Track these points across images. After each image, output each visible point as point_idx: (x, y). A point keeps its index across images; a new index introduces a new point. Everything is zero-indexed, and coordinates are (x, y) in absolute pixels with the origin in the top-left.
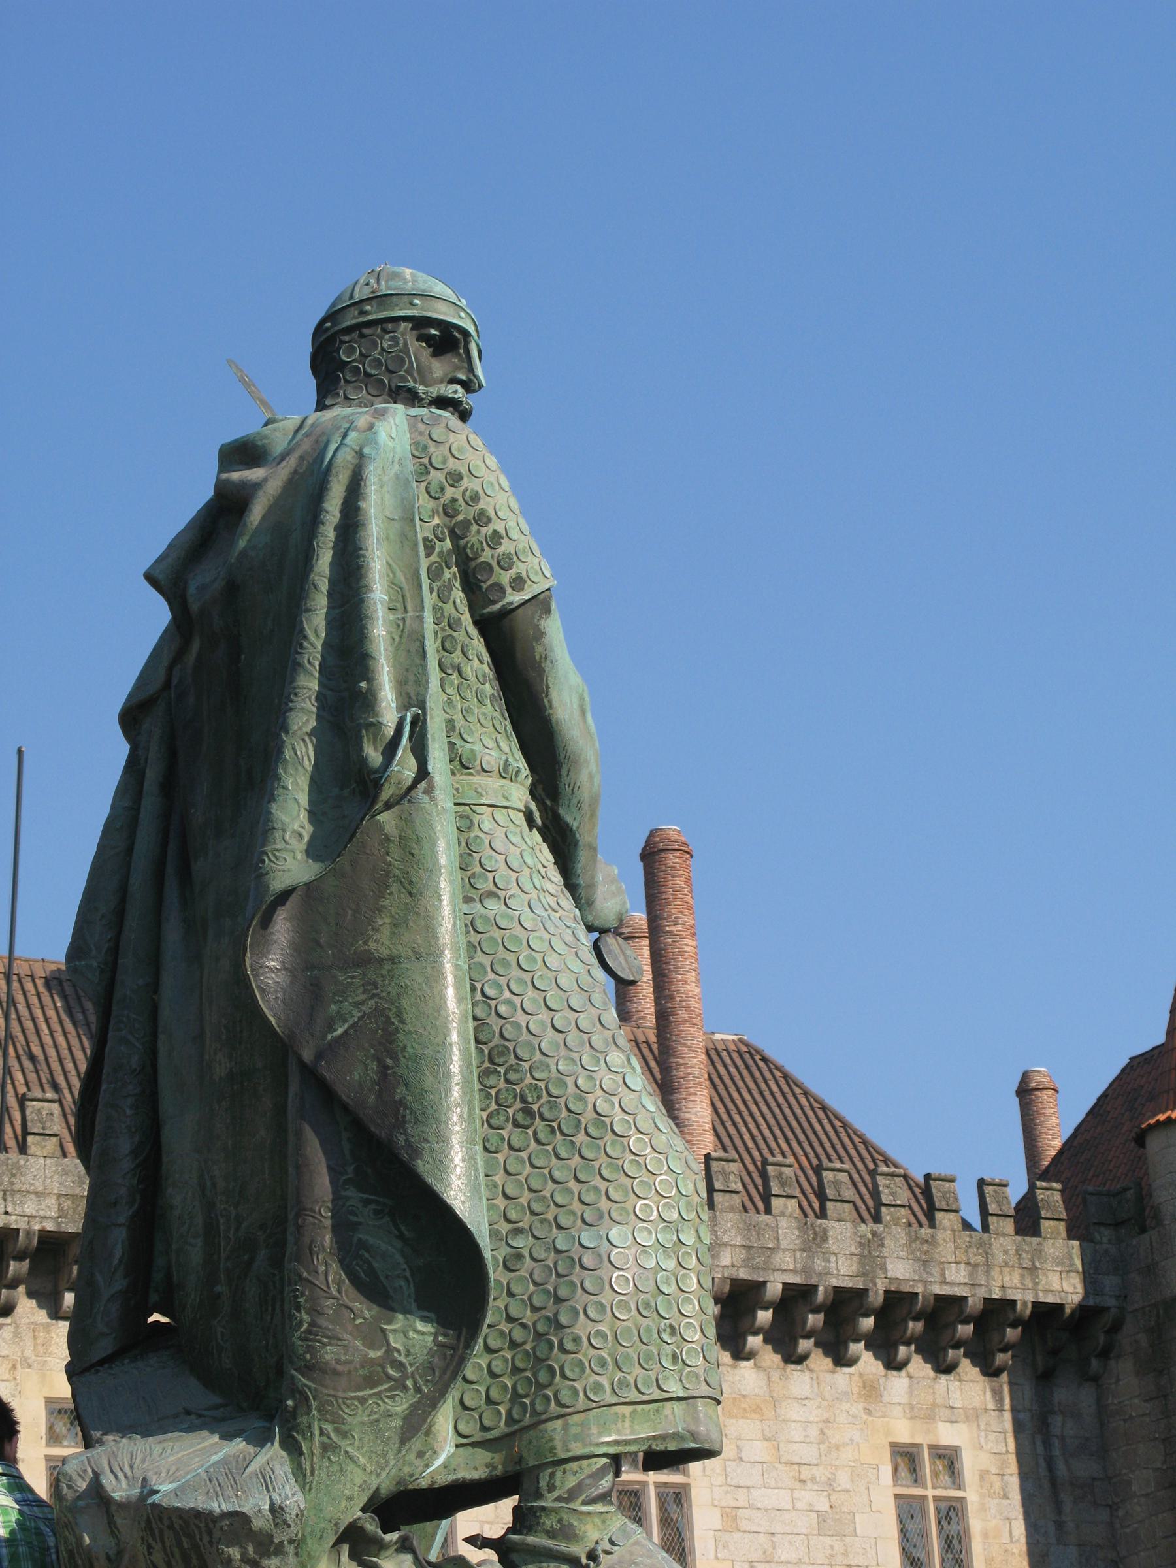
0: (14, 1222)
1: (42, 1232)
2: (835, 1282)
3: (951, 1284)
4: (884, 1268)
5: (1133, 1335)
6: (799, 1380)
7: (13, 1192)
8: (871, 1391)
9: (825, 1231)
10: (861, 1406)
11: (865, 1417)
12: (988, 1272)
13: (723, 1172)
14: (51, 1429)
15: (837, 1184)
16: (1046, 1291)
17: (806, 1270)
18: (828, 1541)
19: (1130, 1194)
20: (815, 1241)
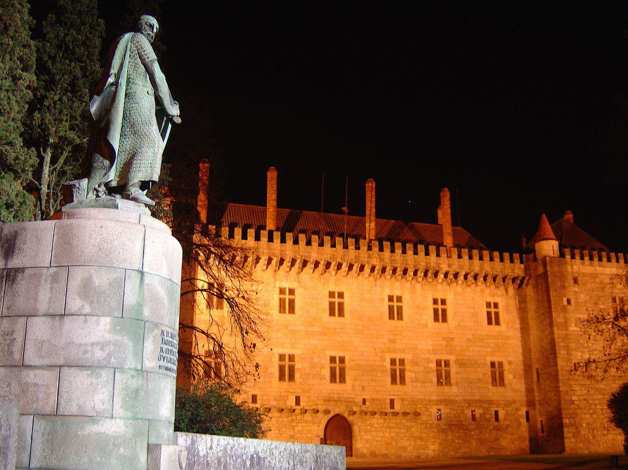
6: (469, 289)
8: (482, 291)
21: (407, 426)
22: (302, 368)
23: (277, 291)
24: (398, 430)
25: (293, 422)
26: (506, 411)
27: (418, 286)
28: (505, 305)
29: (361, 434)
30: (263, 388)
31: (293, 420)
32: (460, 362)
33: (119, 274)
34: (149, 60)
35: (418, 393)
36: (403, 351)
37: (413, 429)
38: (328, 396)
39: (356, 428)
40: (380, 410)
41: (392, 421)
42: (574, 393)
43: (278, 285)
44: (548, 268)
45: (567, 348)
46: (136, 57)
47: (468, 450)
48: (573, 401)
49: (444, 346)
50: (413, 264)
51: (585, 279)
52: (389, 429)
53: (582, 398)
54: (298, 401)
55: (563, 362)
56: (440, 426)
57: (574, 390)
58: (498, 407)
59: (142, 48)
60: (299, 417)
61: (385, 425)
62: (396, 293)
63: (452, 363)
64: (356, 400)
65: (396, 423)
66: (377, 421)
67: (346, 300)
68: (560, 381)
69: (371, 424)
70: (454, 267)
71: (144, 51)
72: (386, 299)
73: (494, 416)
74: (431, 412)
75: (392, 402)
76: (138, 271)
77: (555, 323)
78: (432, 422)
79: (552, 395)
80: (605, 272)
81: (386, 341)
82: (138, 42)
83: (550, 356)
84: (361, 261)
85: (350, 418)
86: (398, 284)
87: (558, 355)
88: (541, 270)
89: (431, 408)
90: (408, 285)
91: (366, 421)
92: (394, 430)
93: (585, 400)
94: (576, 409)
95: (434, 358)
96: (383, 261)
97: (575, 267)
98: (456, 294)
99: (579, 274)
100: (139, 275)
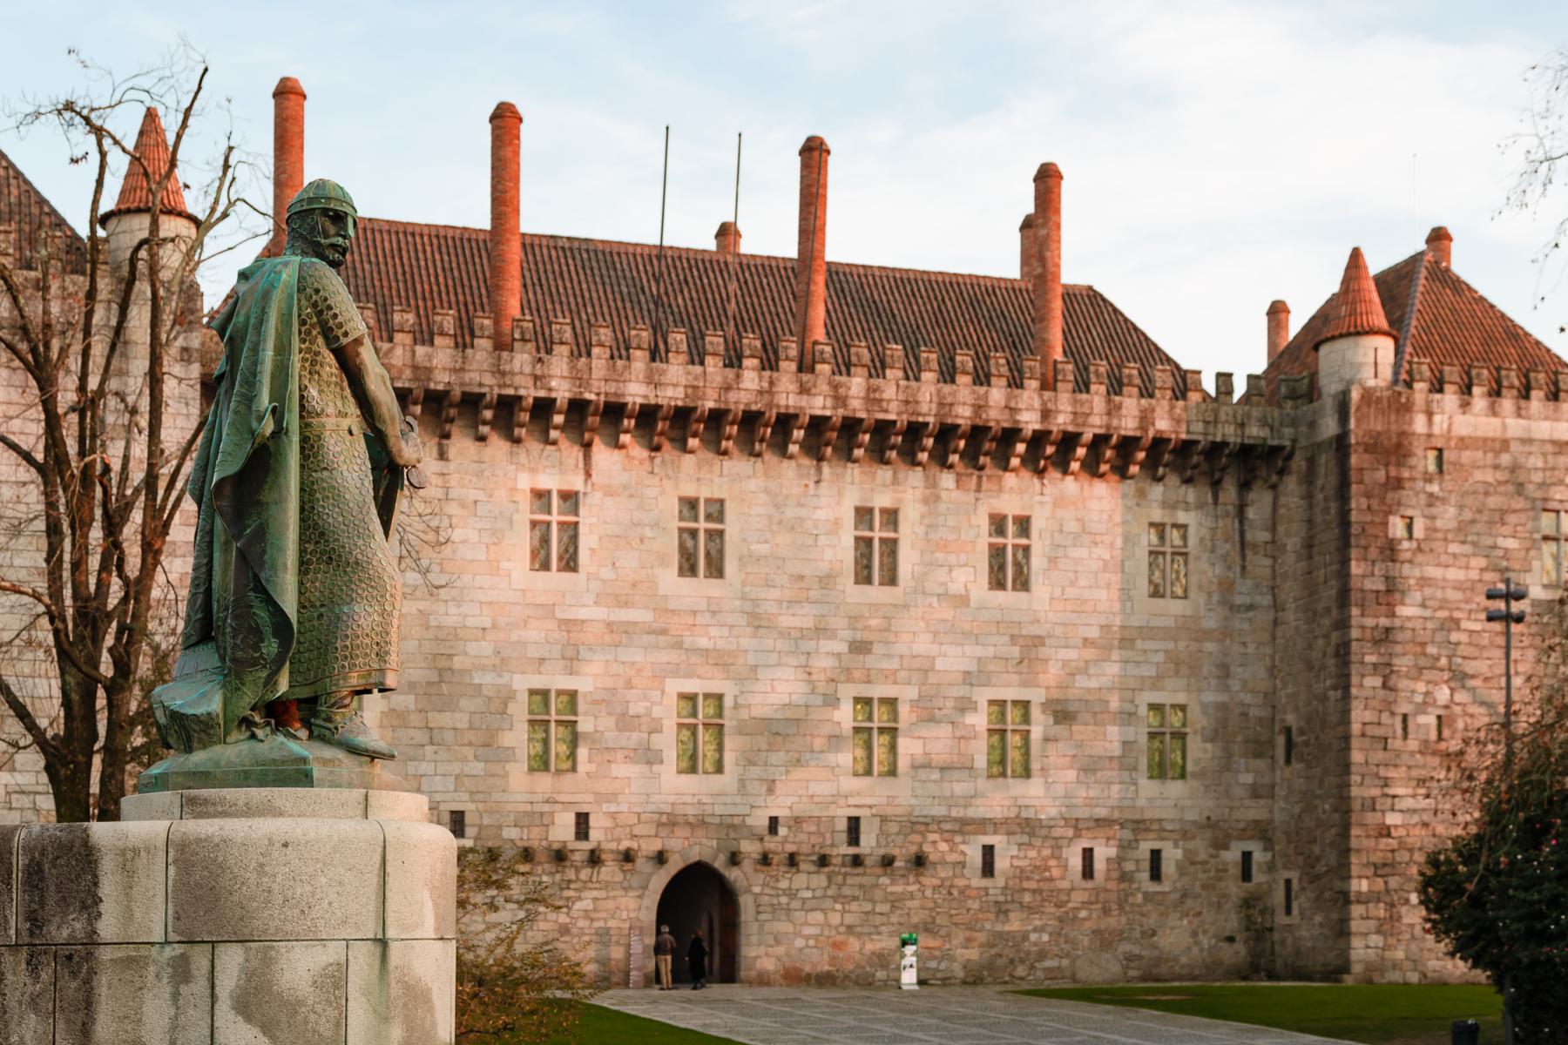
0: (660, 401)
1: (677, 407)
2: (1123, 432)
3: (1193, 433)
4: (1153, 424)
5: (1299, 462)
7: (661, 384)
8: (1141, 494)
9: (1121, 403)
11: (1136, 508)
12: (1215, 426)
13: (1063, 370)
14: (681, 512)
15: (1130, 376)
16: (1249, 437)
17: (1108, 427)
18: (1107, 575)
20: (1113, 410)
21: (892, 893)
22: (596, 731)
23: (525, 501)
24: (868, 907)
25: (568, 888)
26: (1186, 851)
27: (947, 480)
28: (1208, 537)
29: (763, 917)
30: (482, 792)
31: (569, 881)
32: (1059, 708)
33: (334, 952)
34: (350, 339)
35: (930, 800)
36: (891, 677)
37: (909, 904)
38: (669, 810)
39: (746, 903)
40: (817, 848)
41: (850, 881)
42: (1393, 804)
43: (525, 482)
44: (1352, 424)
45: (1386, 671)
46: (314, 332)
47: (1065, 962)
48: (1388, 828)
49: (1015, 662)
50: (933, 412)
51: (1466, 456)
52: (842, 903)
53: (1415, 819)
54: (582, 821)
55: (1367, 713)
56: (987, 894)
57: (1394, 797)
58: (1163, 839)
59: (330, 308)
60: (585, 873)
61: (830, 893)
62: (881, 500)
63: (1036, 713)
64: (749, 821)
65: (861, 886)
66: (807, 881)
67: (732, 527)
68: (1353, 769)
69: (790, 889)
70: (1061, 419)
71: (335, 316)
72: (849, 517)
73: (1146, 865)
74: (963, 853)
75: (854, 825)
76: (375, 940)
77: (1354, 596)
79: (1327, 807)
80: (1535, 436)
81: (842, 647)
82: (317, 291)
83: (1332, 693)
84: (778, 406)
85: (733, 874)
86: (885, 473)
87: (1354, 691)
88: (1329, 427)
89: (964, 842)
90: (915, 477)
91: (777, 881)
92: (854, 906)
93: (1425, 825)
94: (1393, 851)
95: (983, 696)
96: (845, 405)
97: (1437, 419)
98: (1058, 502)
99: (1449, 439)
100: (378, 950)
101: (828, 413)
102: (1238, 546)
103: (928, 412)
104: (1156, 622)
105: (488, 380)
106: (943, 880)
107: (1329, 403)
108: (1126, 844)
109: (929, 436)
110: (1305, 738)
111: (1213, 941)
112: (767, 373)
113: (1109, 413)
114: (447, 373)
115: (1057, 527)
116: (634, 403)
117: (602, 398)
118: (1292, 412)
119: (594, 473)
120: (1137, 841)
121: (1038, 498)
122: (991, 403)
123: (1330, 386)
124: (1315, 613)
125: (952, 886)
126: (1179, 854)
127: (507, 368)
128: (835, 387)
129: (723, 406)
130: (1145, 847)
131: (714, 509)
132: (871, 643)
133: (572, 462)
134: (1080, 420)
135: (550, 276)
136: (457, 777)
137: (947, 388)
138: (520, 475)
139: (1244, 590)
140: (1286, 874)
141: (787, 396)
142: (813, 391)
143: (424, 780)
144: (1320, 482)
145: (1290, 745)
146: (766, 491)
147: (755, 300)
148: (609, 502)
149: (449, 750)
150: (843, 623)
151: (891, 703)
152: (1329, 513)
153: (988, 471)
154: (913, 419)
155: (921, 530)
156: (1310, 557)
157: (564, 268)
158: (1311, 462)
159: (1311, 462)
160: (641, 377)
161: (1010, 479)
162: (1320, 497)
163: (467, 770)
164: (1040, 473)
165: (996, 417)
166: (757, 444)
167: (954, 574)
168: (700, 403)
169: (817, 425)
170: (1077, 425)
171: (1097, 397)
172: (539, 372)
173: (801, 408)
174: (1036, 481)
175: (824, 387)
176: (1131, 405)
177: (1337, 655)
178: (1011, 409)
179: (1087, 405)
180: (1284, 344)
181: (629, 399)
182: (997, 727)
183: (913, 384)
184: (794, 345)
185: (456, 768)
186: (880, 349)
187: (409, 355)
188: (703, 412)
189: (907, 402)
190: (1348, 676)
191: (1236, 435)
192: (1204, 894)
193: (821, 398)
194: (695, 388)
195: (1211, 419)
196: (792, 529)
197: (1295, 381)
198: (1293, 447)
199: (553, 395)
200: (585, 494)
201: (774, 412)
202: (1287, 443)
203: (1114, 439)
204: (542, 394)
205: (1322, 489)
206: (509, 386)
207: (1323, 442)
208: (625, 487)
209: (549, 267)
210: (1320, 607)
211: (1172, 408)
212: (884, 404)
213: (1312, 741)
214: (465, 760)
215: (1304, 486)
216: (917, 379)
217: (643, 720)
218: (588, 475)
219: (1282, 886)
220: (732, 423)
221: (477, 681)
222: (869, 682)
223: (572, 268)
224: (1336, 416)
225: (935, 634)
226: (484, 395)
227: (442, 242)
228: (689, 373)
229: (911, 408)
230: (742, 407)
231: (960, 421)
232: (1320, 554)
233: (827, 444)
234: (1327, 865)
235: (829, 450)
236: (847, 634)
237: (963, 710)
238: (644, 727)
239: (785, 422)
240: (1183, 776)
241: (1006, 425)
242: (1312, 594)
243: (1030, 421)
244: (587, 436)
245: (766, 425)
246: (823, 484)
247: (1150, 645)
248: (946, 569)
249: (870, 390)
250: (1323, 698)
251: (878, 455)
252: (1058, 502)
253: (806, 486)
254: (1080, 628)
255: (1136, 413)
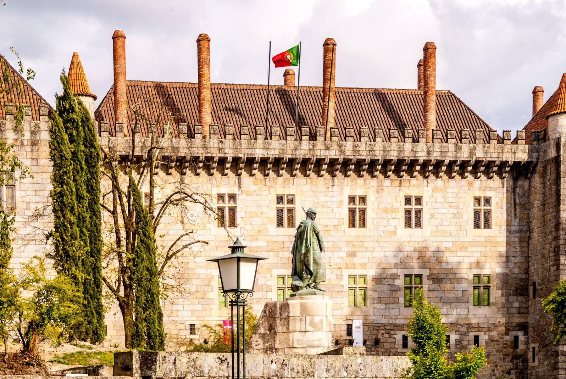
1: (275, 158)
2: (462, 159)
4: (475, 155)
5: (539, 168)
8: (470, 184)
10: (467, 188)
11: (468, 191)
16: (517, 158)
17: (456, 157)
18: (456, 220)
19: (543, 133)
20: (458, 149)
26: (489, 335)
27: (387, 182)
35: (381, 317)
49: (416, 258)
58: (480, 331)
62: (359, 192)
63: (425, 279)
70: (435, 155)
72: (346, 200)
78: (396, 350)
81: (344, 255)
83: (552, 268)
84: (317, 156)
86: (360, 181)
88: (552, 153)
96: (344, 154)
98: (435, 190)
101: (337, 157)
102: (513, 205)
103: (379, 155)
104: (477, 239)
105: (201, 151)
106: (386, 350)
107: (552, 143)
108: (463, 333)
109: (379, 165)
110: (541, 287)
111: (501, 374)
112: (312, 142)
113: (456, 151)
114: (185, 149)
115: (434, 201)
116: (259, 157)
117: (246, 156)
118: (537, 147)
119: (242, 186)
120: (468, 332)
121: (426, 188)
122: (405, 150)
123: (552, 136)
124: (546, 233)
125: (390, 352)
126: (486, 337)
127: (208, 146)
128: (340, 146)
129: (294, 157)
130: (472, 335)
131: (290, 197)
132: (356, 252)
133: (233, 182)
134: (443, 155)
135: (220, 102)
136: (192, 311)
137: (387, 144)
138: (213, 188)
139: (515, 224)
140: (532, 345)
141: (320, 151)
142: (331, 148)
143: (179, 312)
144: (548, 177)
145: (535, 290)
146: (312, 190)
147: (304, 107)
148: (248, 198)
149: (189, 300)
150: (344, 244)
151: (364, 277)
152: (552, 191)
153: (404, 178)
154: (373, 158)
155: (376, 205)
156: (544, 210)
157: (225, 98)
158: (545, 168)
159: (545, 168)
160: (261, 146)
161: (414, 181)
162: (548, 183)
163: (196, 308)
164: (426, 177)
165: (407, 155)
166: (308, 172)
167: (390, 222)
168: (285, 156)
169: (333, 163)
170: (442, 157)
171: (451, 145)
172: (221, 147)
173: (326, 156)
174: (425, 180)
175: (335, 146)
176: (466, 147)
177: (554, 251)
178: (414, 151)
179: (447, 148)
180: (538, 110)
181: (257, 156)
182: (409, 286)
183: (373, 143)
184: (323, 129)
185: (191, 307)
186: (359, 129)
187: (170, 142)
188: (286, 159)
189: (370, 151)
190: (559, 260)
191: (512, 157)
192: (497, 354)
193: (334, 151)
194: (283, 150)
195: (501, 151)
196: (323, 206)
197: (538, 132)
198: (537, 162)
199: (226, 156)
200: (239, 195)
201: (315, 158)
202: (535, 160)
203: (458, 163)
204: (222, 155)
205: (549, 180)
206: (209, 153)
207: (549, 160)
208: (255, 191)
209: (219, 98)
210: (548, 231)
211: (484, 147)
212: (361, 153)
213: (544, 288)
214: (195, 304)
215: (542, 179)
216: (374, 141)
217: (264, 286)
218: (240, 187)
219: (531, 350)
220: (298, 164)
221: (198, 272)
222: (355, 268)
223: (228, 98)
224: (555, 148)
225: (382, 247)
226: (199, 157)
227: (175, 90)
228: (280, 144)
229: (372, 153)
230: (302, 157)
231: (392, 158)
232: (548, 208)
233: (337, 170)
234: (549, 340)
235: (338, 172)
236: (346, 249)
237: (394, 279)
238: (264, 290)
239: (319, 162)
240: (488, 304)
241: (412, 158)
242: (544, 226)
243: (422, 156)
244: (239, 171)
245: (311, 164)
246: (334, 187)
247: (474, 249)
248: (387, 220)
249: (355, 146)
250: (549, 270)
251: (358, 172)
252: (435, 190)
253: (328, 187)
254: (444, 243)
255: (468, 150)
